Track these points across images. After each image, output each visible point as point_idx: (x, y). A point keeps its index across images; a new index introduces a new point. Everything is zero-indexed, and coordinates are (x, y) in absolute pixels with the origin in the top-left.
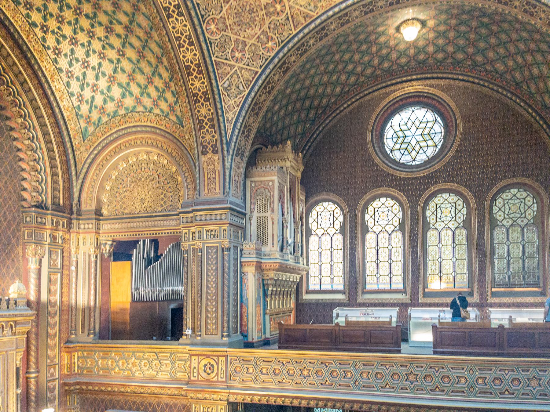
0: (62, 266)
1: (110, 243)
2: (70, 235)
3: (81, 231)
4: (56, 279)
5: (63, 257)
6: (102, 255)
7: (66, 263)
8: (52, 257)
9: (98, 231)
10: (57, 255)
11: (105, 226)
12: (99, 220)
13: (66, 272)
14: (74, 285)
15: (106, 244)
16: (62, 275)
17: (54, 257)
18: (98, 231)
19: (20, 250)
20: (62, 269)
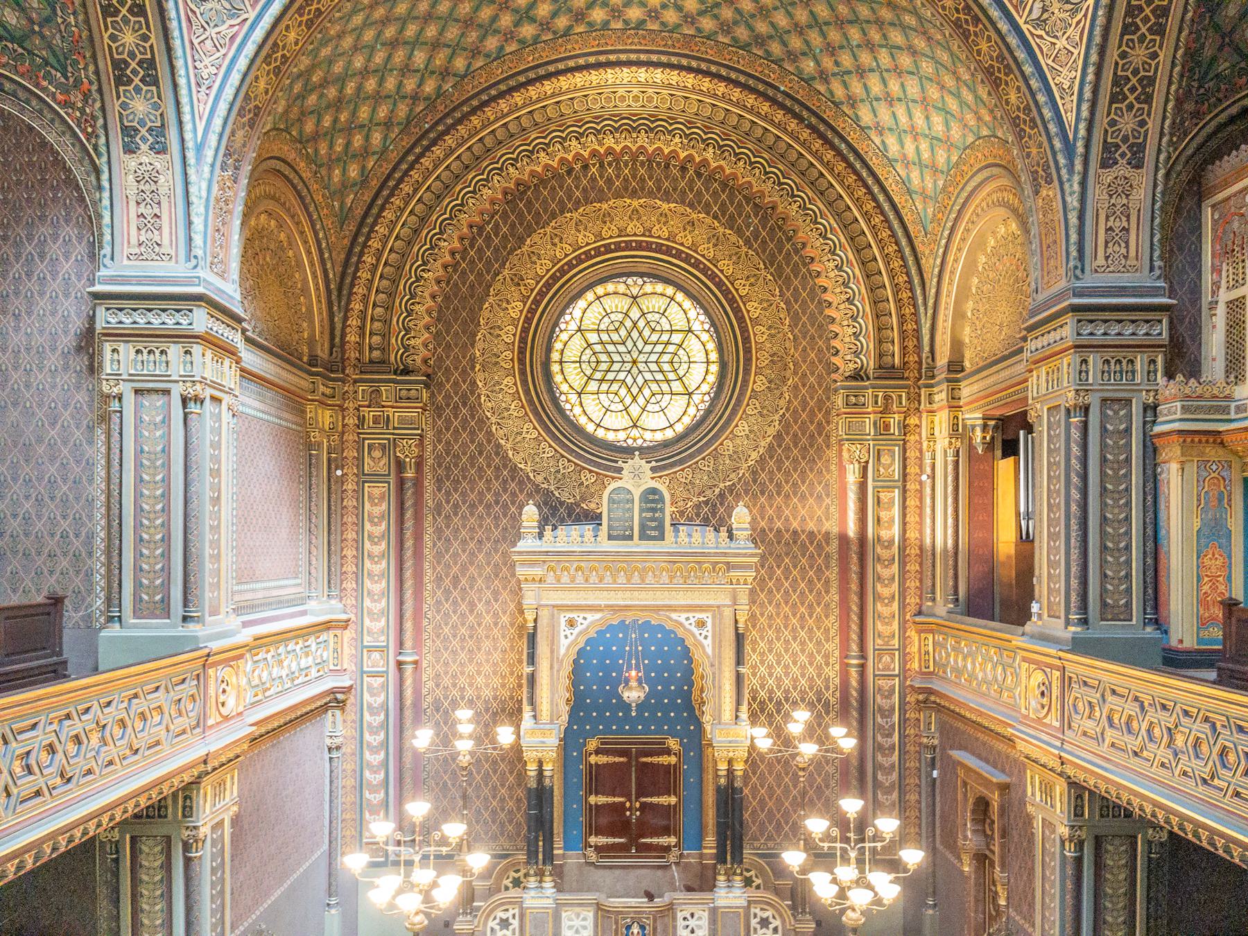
0: (905, 475)
1: (980, 422)
2: (920, 418)
3: (935, 406)
4: (892, 500)
5: (905, 459)
7: (912, 469)
8: (882, 460)
9: (955, 403)
10: (893, 457)
11: (967, 390)
12: (958, 380)
13: (911, 486)
14: (928, 511)
15: (973, 427)
16: (904, 491)
17: (885, 459)
18: (955, 403)
19: (832, 453)
20: (905, 481)
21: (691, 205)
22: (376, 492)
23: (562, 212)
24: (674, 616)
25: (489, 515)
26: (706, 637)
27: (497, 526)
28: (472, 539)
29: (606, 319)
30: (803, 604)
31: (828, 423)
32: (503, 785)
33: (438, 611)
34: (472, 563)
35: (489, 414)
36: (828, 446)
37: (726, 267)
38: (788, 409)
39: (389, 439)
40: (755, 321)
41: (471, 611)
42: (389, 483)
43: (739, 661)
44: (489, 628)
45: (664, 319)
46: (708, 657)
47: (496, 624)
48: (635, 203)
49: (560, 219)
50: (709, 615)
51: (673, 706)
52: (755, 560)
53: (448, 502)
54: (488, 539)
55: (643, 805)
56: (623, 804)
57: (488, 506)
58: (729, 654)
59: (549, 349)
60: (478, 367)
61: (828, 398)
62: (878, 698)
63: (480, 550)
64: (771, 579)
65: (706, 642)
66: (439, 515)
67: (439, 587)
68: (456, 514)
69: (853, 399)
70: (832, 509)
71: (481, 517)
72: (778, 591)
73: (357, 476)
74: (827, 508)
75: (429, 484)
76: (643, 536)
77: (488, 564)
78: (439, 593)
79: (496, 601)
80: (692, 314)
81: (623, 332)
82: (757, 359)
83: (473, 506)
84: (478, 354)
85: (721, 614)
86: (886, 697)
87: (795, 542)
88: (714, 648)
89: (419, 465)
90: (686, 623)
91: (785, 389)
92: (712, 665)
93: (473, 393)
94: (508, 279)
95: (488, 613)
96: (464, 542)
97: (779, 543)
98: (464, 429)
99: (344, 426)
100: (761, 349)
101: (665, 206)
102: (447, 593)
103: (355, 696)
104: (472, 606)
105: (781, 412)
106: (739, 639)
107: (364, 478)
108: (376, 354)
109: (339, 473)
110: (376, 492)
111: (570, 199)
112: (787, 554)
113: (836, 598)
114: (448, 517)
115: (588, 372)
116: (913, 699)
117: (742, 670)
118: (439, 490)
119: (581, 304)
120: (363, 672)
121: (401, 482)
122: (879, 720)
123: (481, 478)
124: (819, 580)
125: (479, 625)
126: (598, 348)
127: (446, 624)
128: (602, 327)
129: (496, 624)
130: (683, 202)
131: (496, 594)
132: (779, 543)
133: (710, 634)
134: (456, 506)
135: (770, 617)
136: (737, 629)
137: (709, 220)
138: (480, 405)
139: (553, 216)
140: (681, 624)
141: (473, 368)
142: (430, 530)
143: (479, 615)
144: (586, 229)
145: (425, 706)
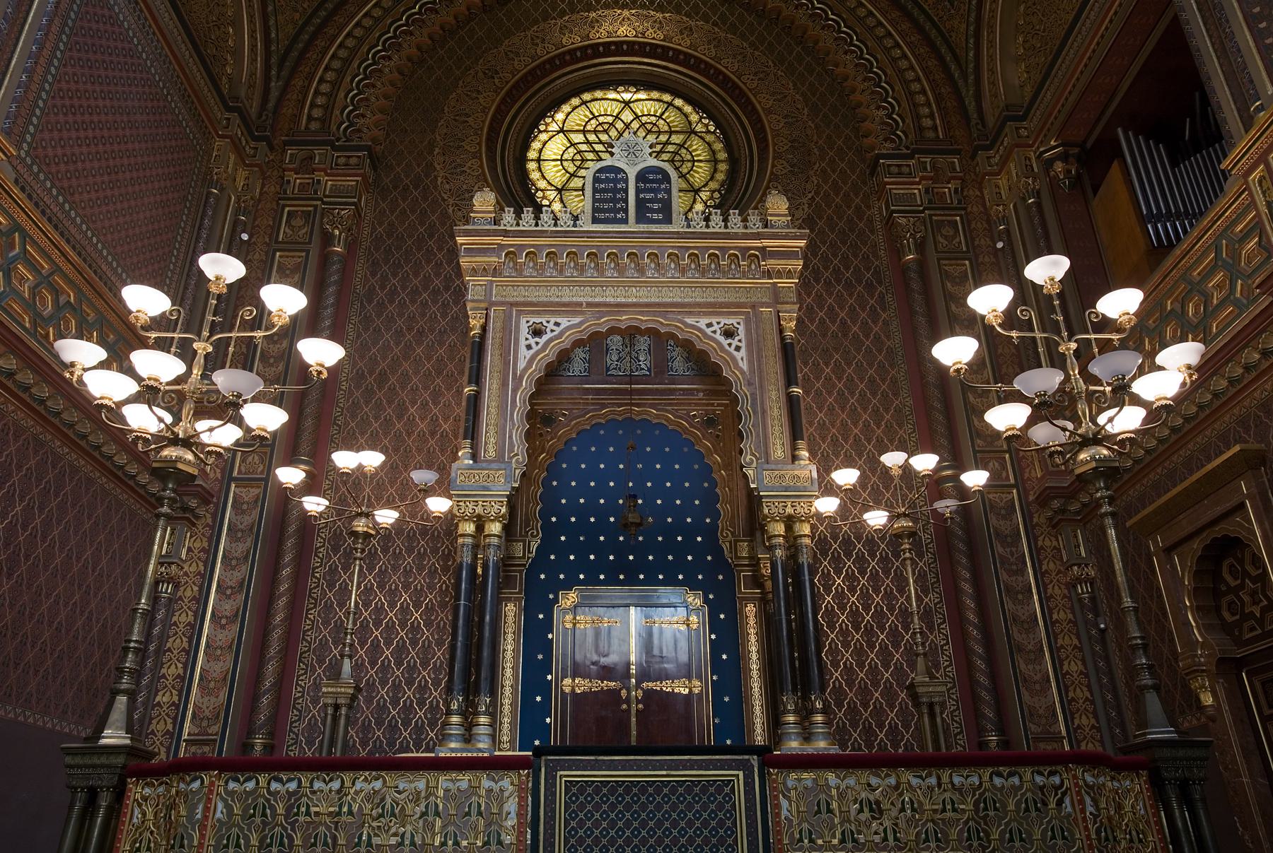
6: (1053, 184)
21: (687, 15)
22: (289, 263)
23: (545, 20)
24: (689, 321)
25: (435, 302)
26: (738, 349)
27: (444, 315)
28: (410, 329)
29: (593, 122)
30: (865, 410)
31: (869, 207)
32: (425, 664)
33: (353, 417)
34: (406, 358)
35: (445, 197)
36: (872, 232)
37: (728, 66)
38: (817, 193)
39: (316, 207)
40: (769, 112)
41: (400, 417)
42: (308, 252)
43: (790, 380)
44: (422, 436)
45: (661, 122)
46: (742, 372)
47: (433, 434)
48: (626, 13)
49: (542, 25)
50: (741, 319)
51: (690, 546)
52: (802, 243)
53: (383, 287)
54: (432, 330)
55: (649, 694)
56: (614, 693)
57: (436, 292)
58: (774, 368)
59: (526, 147)
60: (437, 150)
61: (865, 183)
62: (993, 520)
63: (419, 343)
64: (818, 379)
65: (738, 355)
66: (370, 302)
67: (358, 387)
68: (391, 301)
69: (895, 170)
70: (888, 298)
71: (424, 305)
72: (830, 393)
73: (268, 245)
74: (882, 297)
75: (361, 268)
76: (640, 219)
77: (429, 359)
78: (357, 394)
79: (435, 404)
80: (694, 118)
81: (613, 133)
82: (775, 145)
83: (415, 293)
84: (438, 138)
85: (758, 315)
86: (1004, 517)
87: (845, 335)
88: (750, 362)
89: (351, 246)
90: (709, 331)
91: (811, 173)
92: (750, 384)
93: (427, 176)
94: (480, 74)
95: (422, 419)
96: (399, 333)
97: (824, 336)
98: (413, 212)
99: (261, 194)
100: (778, 135)
101: (659, 15)
102: (369, 393)
103: (214, 516)
104: (401, 411)
105: (810, 196)
106: (787, 350)
107: (275, 246)
108: (314, 126)
109: (245, 237)
110: (289, 263)
111: (554, 10)
112: (836, 350)
113: (909, 401)
114: (381, 306)
115: (572, 169)
116: (1043, 520)
117: (797, 390)
118: (374, 274)
119: (566, 108)
120: (231, 479)
121: (325, 260)
122: (1001, 550)
123: (429, 262)
124: (883, 380)
125: (409, 435)
126: (584, 147)
127: (362, 434)
128: (589, 128)
129: (433, 434)
130: (679, 13)
131: (436, 395)
132: (824, 336)
133: (743, 345)
134: (393, 293)
135: (822, 426)
136: (783, 339)
137: (708, 27)
138: (435, 187)
139: (536, 22)
140: (700, 330)
141: (431, 152)
142: (355, 319)
143: (411, 421)
144: (571, 32)
145: (318, 543)
